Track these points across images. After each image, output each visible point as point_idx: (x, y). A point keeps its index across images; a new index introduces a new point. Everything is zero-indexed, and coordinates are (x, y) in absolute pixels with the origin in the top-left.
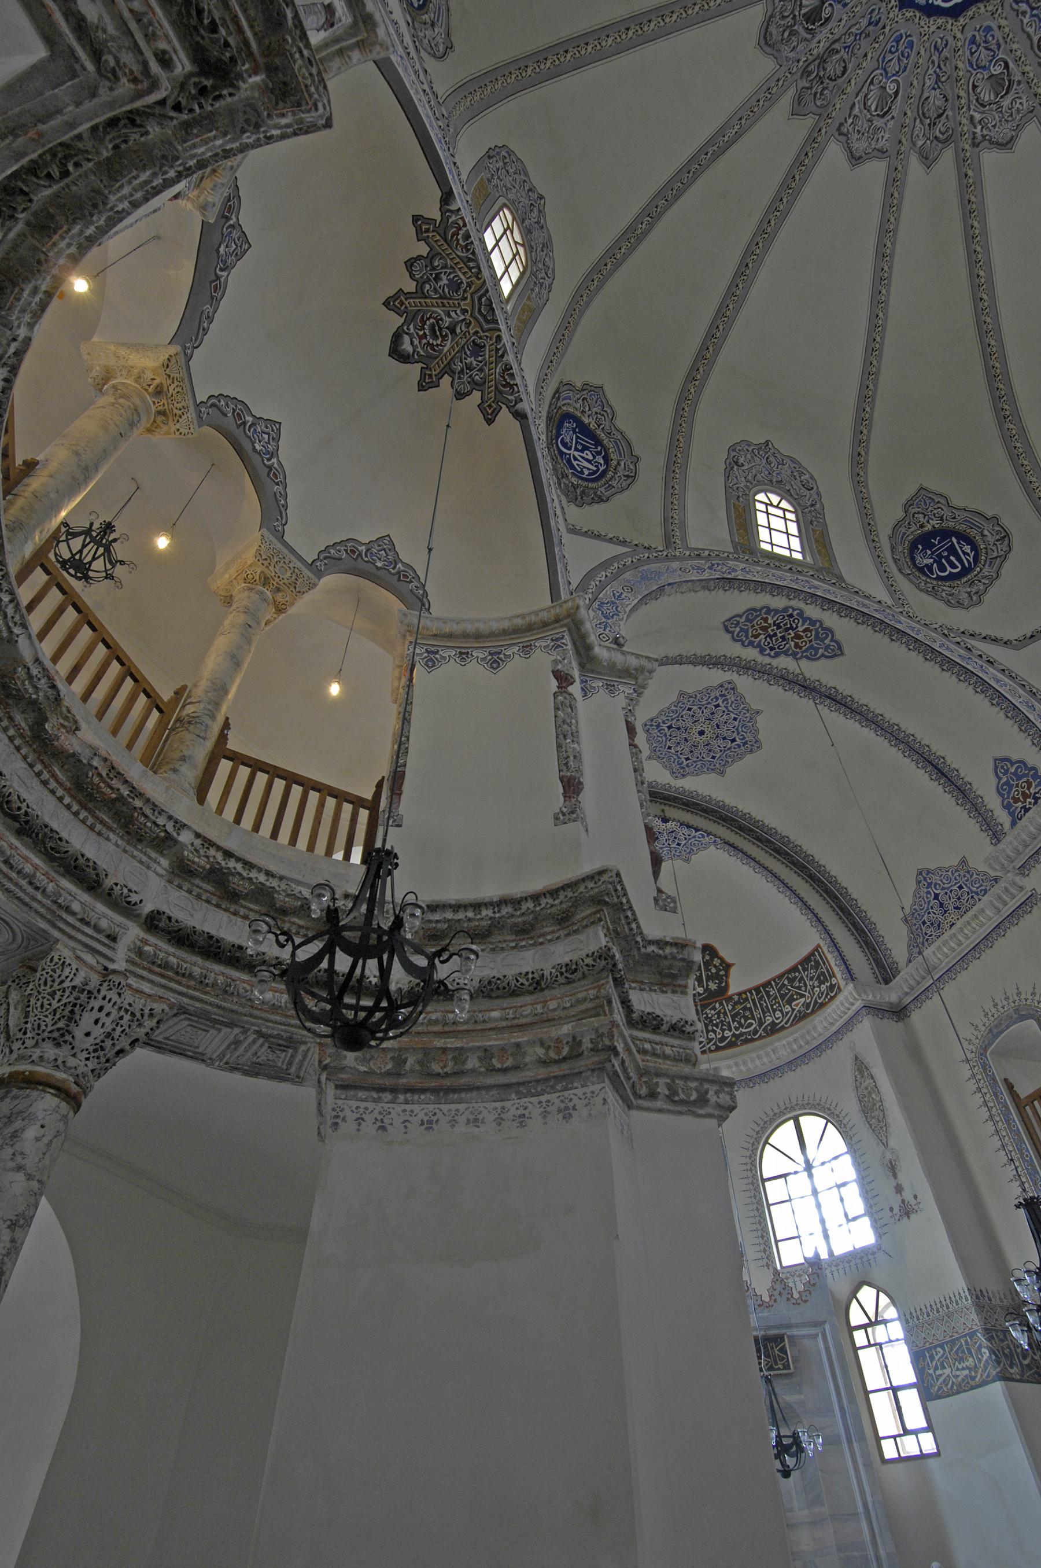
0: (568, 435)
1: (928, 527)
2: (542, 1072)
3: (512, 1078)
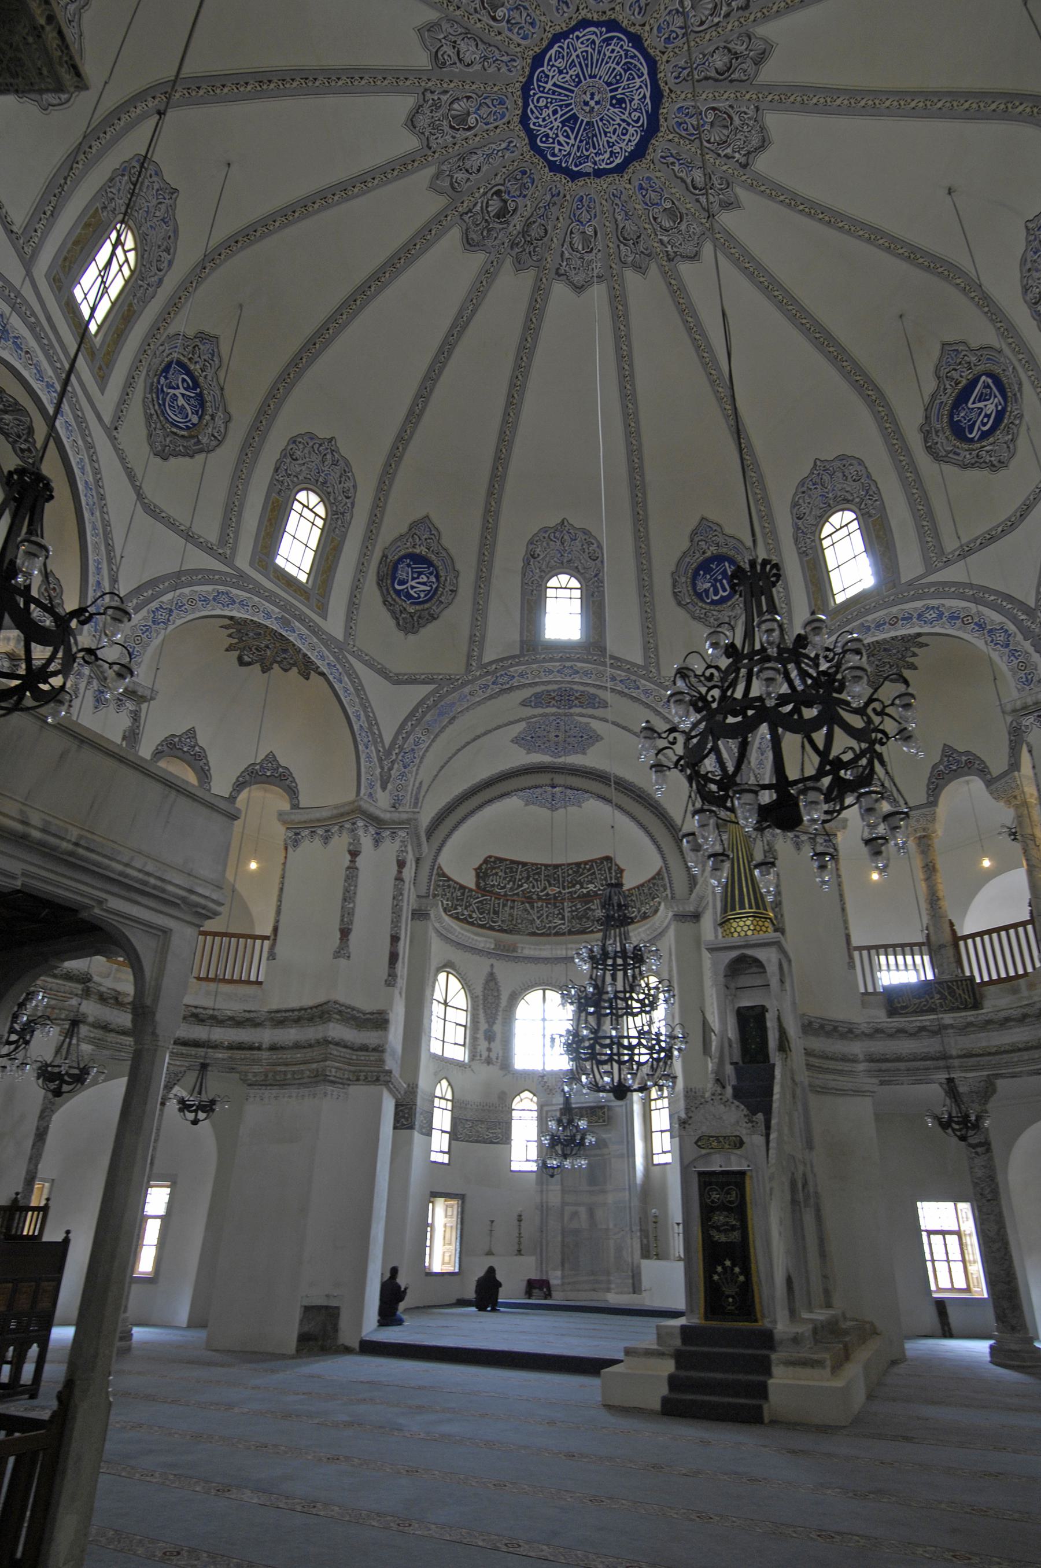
0: (401, 574)
1: (709, 554)
2: (309, 1080)
3: (301, 1081)
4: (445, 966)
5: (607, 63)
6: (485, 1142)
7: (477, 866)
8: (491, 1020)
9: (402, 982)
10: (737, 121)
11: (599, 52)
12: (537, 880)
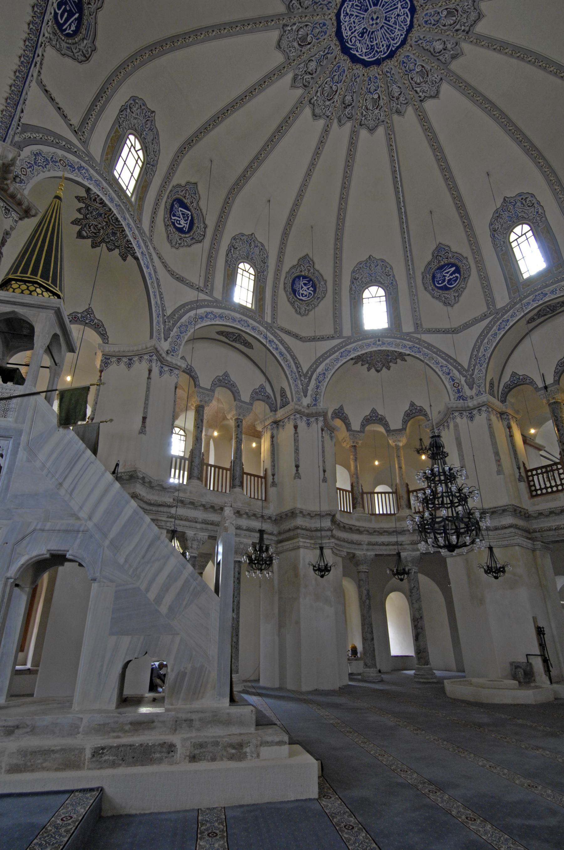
5: (381, 39)
10: (328, 103)
11: (388, 39)
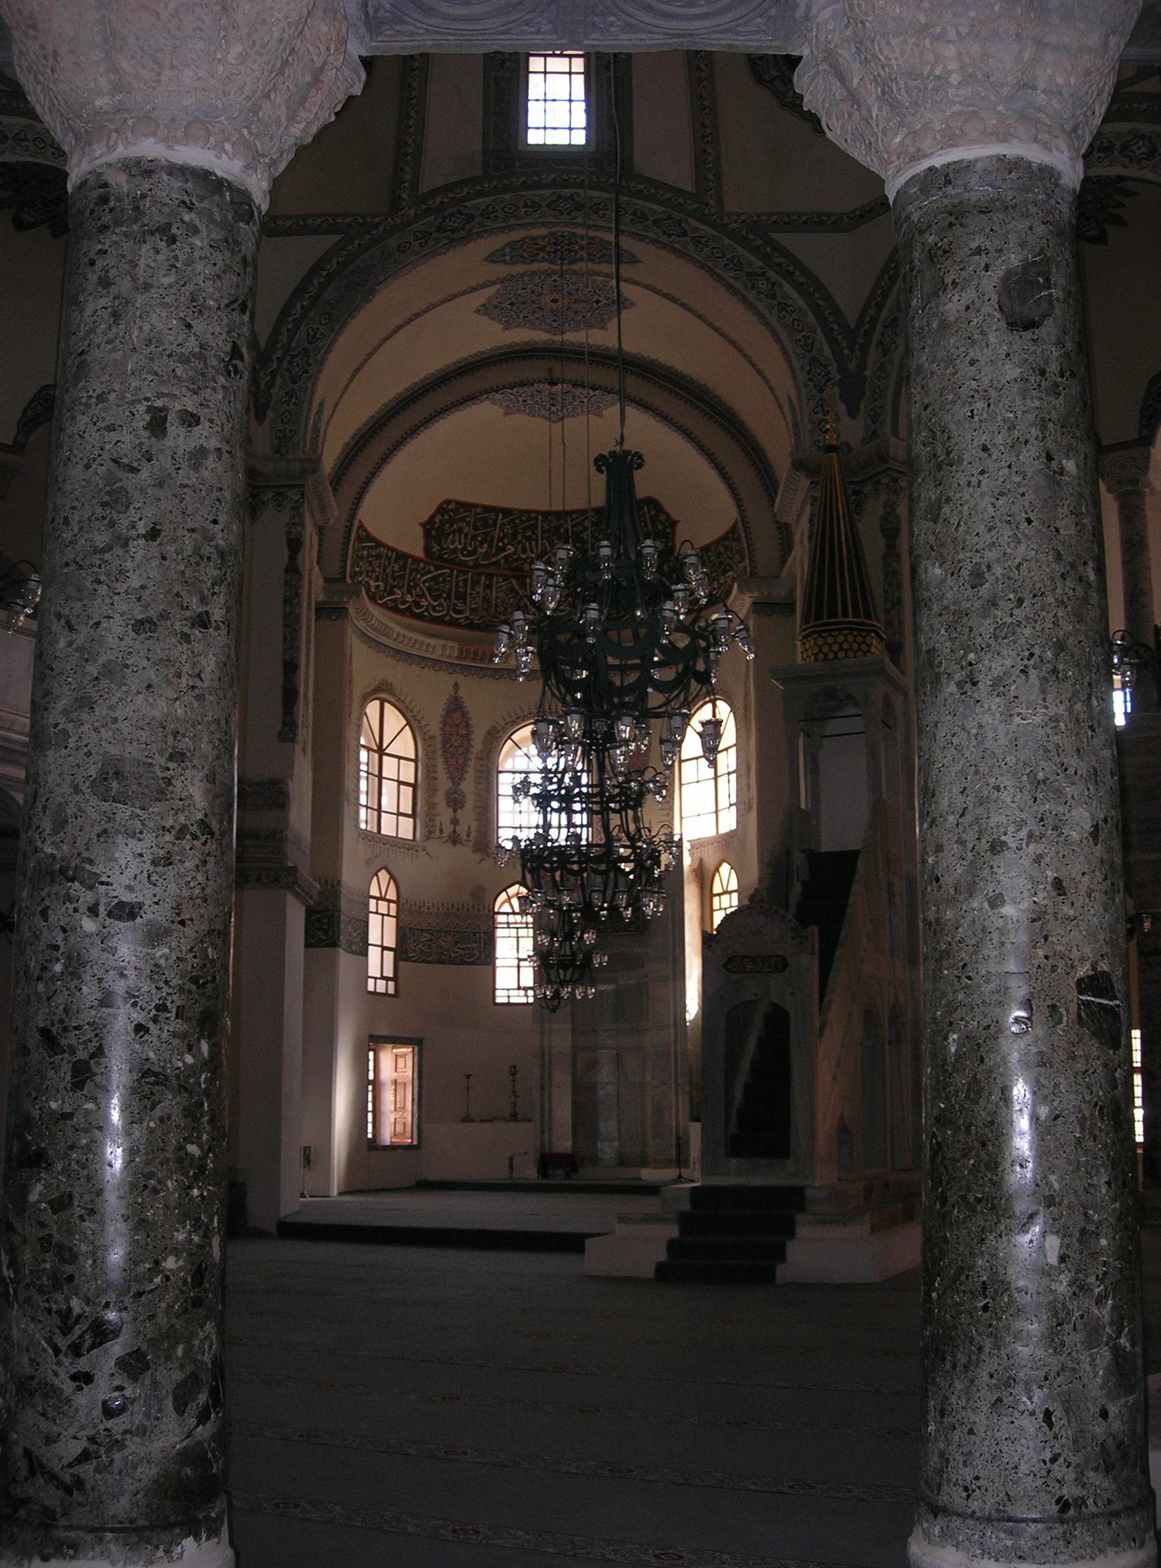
4: (377, 690)
6: (452, 963)
7: (425, 518)
8: (457, 772)
9: (305, 733)
12: (529, 539)
